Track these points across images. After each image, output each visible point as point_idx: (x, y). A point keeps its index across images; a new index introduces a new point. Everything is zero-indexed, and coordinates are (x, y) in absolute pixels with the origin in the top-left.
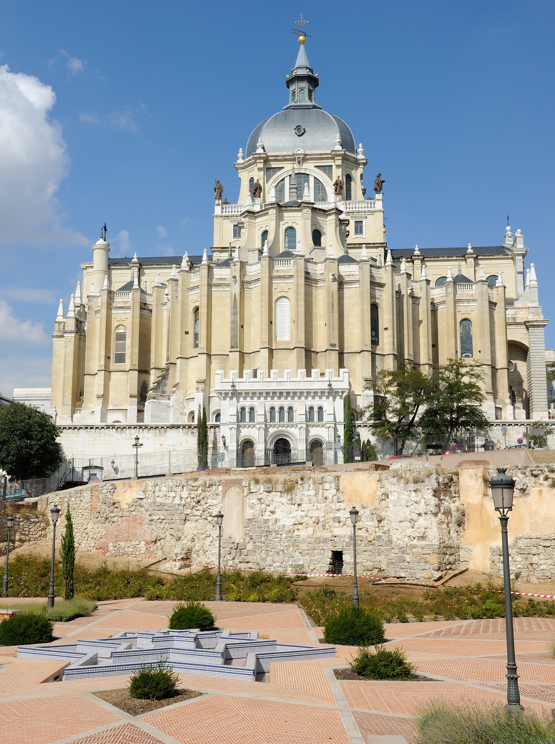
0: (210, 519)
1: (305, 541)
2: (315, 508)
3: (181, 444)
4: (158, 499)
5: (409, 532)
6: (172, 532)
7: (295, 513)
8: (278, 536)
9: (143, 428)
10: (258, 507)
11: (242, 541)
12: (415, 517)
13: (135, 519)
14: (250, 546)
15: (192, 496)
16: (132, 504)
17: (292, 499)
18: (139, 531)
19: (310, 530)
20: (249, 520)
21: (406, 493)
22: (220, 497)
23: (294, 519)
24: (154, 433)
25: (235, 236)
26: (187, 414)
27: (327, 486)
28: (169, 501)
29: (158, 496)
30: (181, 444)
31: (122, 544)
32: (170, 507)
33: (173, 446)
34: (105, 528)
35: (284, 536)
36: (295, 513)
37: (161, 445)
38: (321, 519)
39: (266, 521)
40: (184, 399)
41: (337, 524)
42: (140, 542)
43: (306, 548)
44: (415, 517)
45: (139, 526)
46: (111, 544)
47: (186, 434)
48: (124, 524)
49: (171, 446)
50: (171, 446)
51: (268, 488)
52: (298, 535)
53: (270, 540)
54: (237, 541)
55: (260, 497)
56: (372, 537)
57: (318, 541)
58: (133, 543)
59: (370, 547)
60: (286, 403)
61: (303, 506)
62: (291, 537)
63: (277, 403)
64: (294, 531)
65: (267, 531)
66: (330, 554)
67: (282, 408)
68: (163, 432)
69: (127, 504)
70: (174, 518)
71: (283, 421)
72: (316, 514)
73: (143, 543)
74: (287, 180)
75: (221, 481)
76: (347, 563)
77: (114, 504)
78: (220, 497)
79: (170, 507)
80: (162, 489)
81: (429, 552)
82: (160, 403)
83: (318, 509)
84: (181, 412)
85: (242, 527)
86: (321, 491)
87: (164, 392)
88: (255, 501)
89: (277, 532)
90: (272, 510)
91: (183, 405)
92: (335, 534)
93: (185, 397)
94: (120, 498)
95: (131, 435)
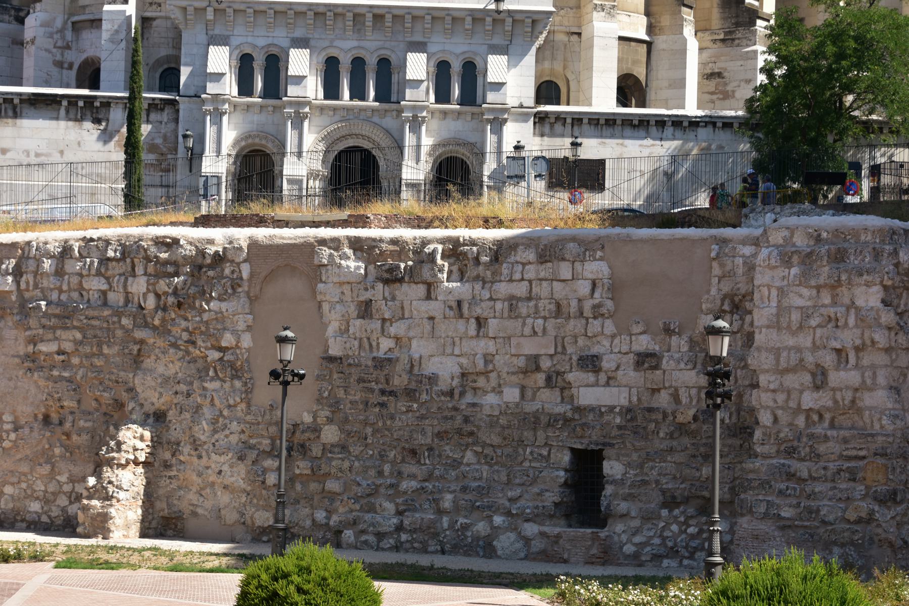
1: (493, 422)
2: (527, 330)
3: (62, 152)
5: (809, 400)
7: (468, 346)
11: (307, 418)
12: (828, 359)
14: (331, 434)
19: (512, 395)
20: (332, 359)
21: (805, 292)
23: (464, 361)
26: (76, 67)
30: (62, 152)
33: (37, 155)
36: (468, 346)
38: (545, 364)
39: (380, 363)
40: (65, 23)
41: (591, 377)
43: (496, 440)
44: (828, 359)
49: (32, 154)
50: (32, 154)
52: (474, 405)
55: (367, 295)
56: (692, 412)
57: (534, 421)
59: (686, 441)
60: (371, 47)
63: (345, 49)
64: (462, 394)
65: (383, 392)
66: (566, 458)
67: (358, 64)
68: (10, 113)
70: (106, 350)
71: (363, 98)
72: (530, 347)
76: (614, 482)
81: (862, 453)
83: (535, 333)
84: (59, 58)
91: (63, 38)
93: (71, 14)
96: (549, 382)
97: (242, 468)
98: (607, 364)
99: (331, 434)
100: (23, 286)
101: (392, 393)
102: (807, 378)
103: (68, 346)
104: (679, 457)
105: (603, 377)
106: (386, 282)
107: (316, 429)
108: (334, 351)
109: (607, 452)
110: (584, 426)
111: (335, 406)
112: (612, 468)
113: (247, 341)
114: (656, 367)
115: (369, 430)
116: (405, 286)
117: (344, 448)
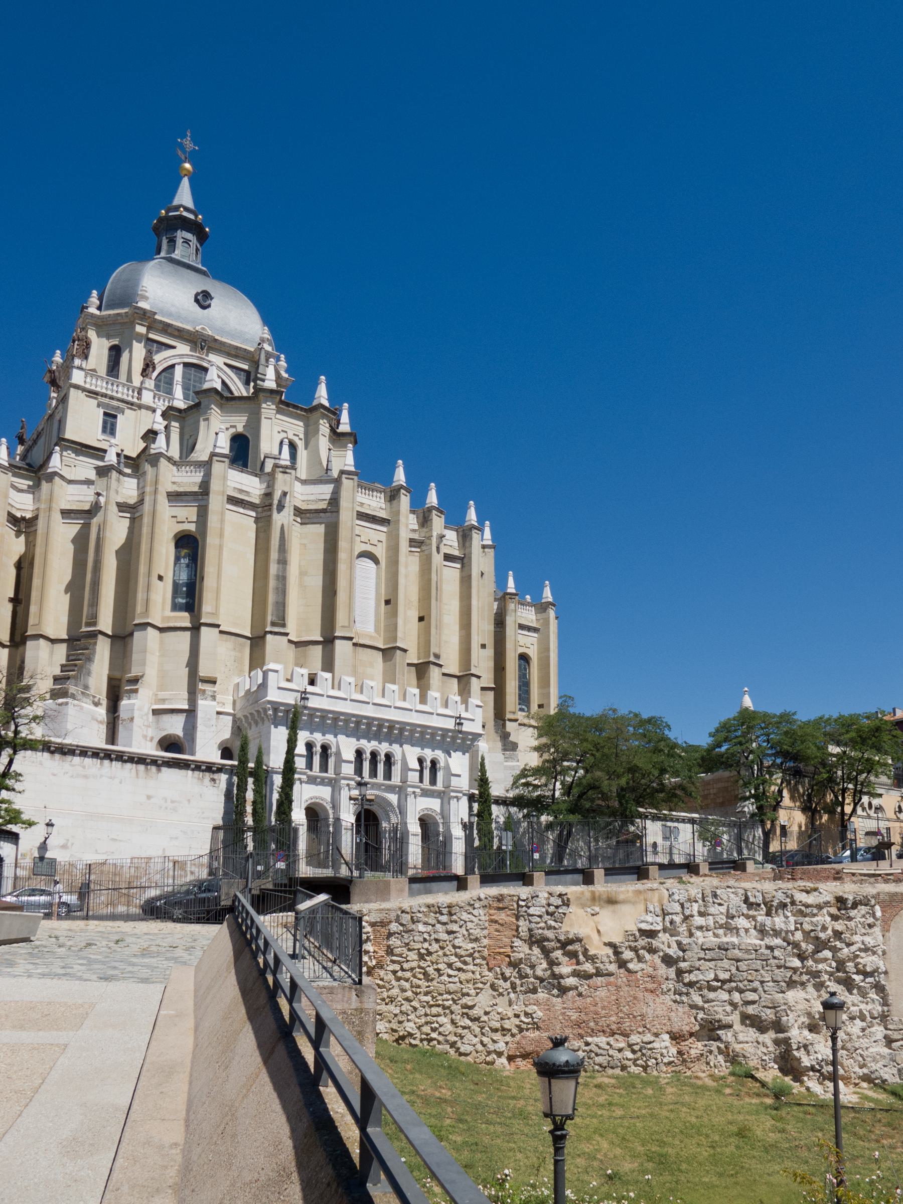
3: (189, 801)
6: (750, 1010)
9: (102, 755)
15: (807, 927)
24: (134, 771)
25: (104, 430)
30: (189, 801)
33: (172, 802)
37: (149, 797)
42: (657, 1035)
47: (201, 780)
58: (635, 1038)
69: (610, 945)
73: (666, 1037)
74: (179, 371)
75: (878, 894)
78: (877, 930)
79: (747, 951)
82: (82, 708)
84: (145, 733)
87: (86, 687)
95: (84, 767)
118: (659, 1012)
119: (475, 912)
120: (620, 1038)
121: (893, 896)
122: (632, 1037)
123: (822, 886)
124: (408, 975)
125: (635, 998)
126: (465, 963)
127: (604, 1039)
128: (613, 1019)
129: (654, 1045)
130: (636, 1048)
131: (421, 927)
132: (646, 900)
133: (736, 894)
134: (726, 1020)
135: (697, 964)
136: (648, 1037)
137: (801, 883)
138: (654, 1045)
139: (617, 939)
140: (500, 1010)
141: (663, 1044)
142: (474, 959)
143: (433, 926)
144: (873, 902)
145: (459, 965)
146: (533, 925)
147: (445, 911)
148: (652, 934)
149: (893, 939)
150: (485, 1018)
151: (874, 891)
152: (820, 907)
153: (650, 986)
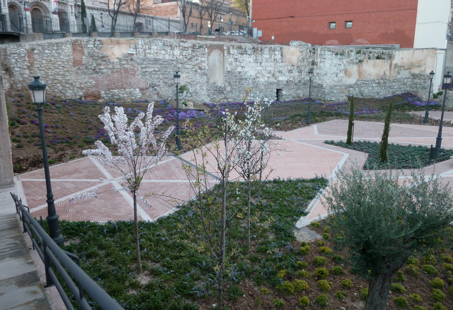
0: (199, 71)
2: (269, 65)
4: (149, 55)
6: (166, 81)
8: (247, 82)
10: (234, 63)
11: (223, 85)
12: (339, 72)
13: (126, 70)
14: (228, 89)
15: (184, 53)
16: (123, 58)
17: (256, 59)
18: (133, 80)
20: (229, 72)
21: (336, 60)
22: (206, 56)
27: (277, 53)
28: (160, 57)
29: (149, 53)
31: (116, 91)
32: (165, 62)
34: (93, 78)
35: (250, 81)
38: (272, 72)
39: (240, 73)
41: (280, 74)
42: (135, 89)
45: (132, 77)
46: (103, 92)
48: (116, 75)
51: (242, 52)
53: (242, 84)
54: (219, 85)
55: (236, 57)
58: (128, 90)
59: (295, 86)
61: (263, 64)
62: (255, 82)
69: (118, 58)
70: (168, 70)
72: (269, 69)
73: (138, 89)
77: (103, 57)
78: (206, 56)
79: (165, 62)
80: (152, 47)
85: (223, 76)
86: (273, 56)
88: (233, 60)
89: (246, 79)
90: (244, 65)
92: (279, 80)
94: (108, 53)
96: (273, 75)
97: (209, 99)
98: (283, 72)
99: (228, 89)
100: (138, 52)
101: (242, 79)
102: (335, 75)
103: (157, 69)
104: (295, 89)
105: (282, 74)
106: (241, 54)
107: (225, 88)
108: (229, 70)
109: (283, 89)
110: (279, 84)
111: (229, 83)
112: (284, 92)
113: (207, 68)
114: (292, 73)
115: (237, 87)
116: (244, 55)
117: (232, 92)
118: (135, 81)
119: (67, 46)
120: (123, 90)
121: (211, 45)
122: (127, 89)
123: (189, 41)
124: (43, 69)
125: (127, 77)
126: (65, 64)
127: (117, 90)
128: (120, 84)
129: (134, 92)
130: (128, 93)
131: (47, 51)
132: (130, 43)
133: (161, 42)
134: (158, 84)
135: (148, 66)
136: (132, 90)
137: (182, 39)
138: (134, 92)
139: (120, 57)
140: (80, 81)
141: (137, 92)
142: (68, 63)
143: (51, 51)
144: (205, 47)
145: (63, 65)
146: (89, 51)
147: (55, 45)
148: (132, 54)
149: (211, 59)
150: (74, 84)
151: (205, 43)
152: (188, 48)
153: (132, 73)
